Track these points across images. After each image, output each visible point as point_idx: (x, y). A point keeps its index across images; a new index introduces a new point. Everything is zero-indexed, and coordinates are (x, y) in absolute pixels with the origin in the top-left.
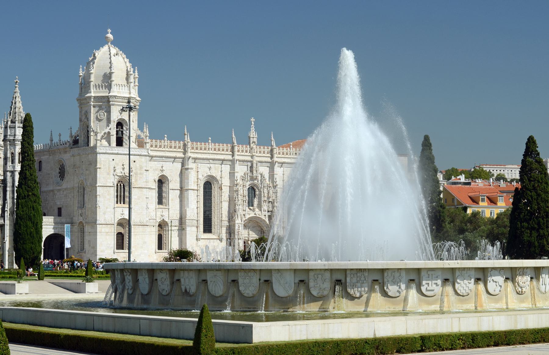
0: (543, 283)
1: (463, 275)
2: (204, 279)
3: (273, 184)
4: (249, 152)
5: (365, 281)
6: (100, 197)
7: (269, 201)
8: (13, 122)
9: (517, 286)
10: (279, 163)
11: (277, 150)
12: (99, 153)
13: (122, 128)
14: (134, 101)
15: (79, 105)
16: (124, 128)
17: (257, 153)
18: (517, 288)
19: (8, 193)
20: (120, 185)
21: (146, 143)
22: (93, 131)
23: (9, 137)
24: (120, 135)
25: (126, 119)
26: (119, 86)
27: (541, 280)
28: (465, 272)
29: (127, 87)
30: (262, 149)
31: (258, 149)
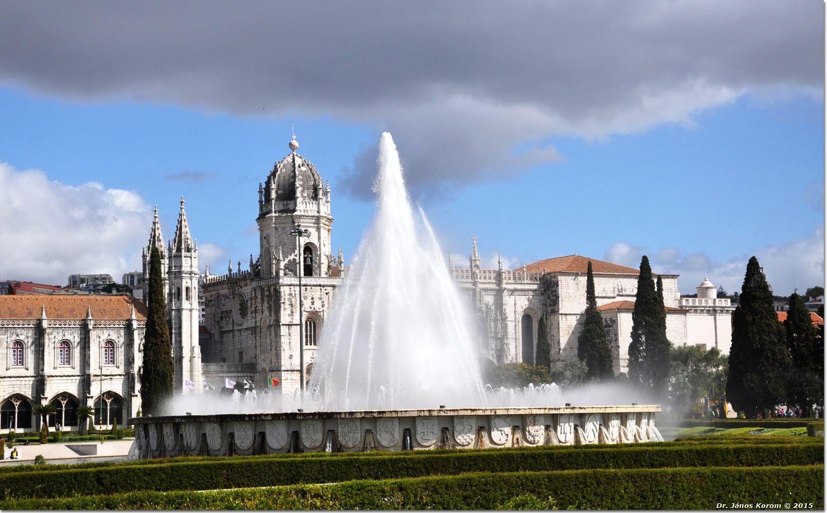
0: (562, 431)
1: (462, 423)
2: (203, 432)
3: (502, 317)
4: (470, 277)
5: (356, 431)
6: (284, 338)
7: (498, 338)
8: (179, 249)
9: (528, 434)
10: (509, 290)
11: (507, 274)
12: (283, 285)
13: (311, 254)
14: (324, 220)
15: (259, 227)
17: (480, 279)
18: (528, 437)
21: (340, 271)
22: (275, 258)
23: (173, 269)
24: (309, 263)
25: (315, 243)
26: (306, 204)
27: (559, 428)
28: (465, 420)
29: (316, 204)
30: (487, 274)
31: (482, 274)
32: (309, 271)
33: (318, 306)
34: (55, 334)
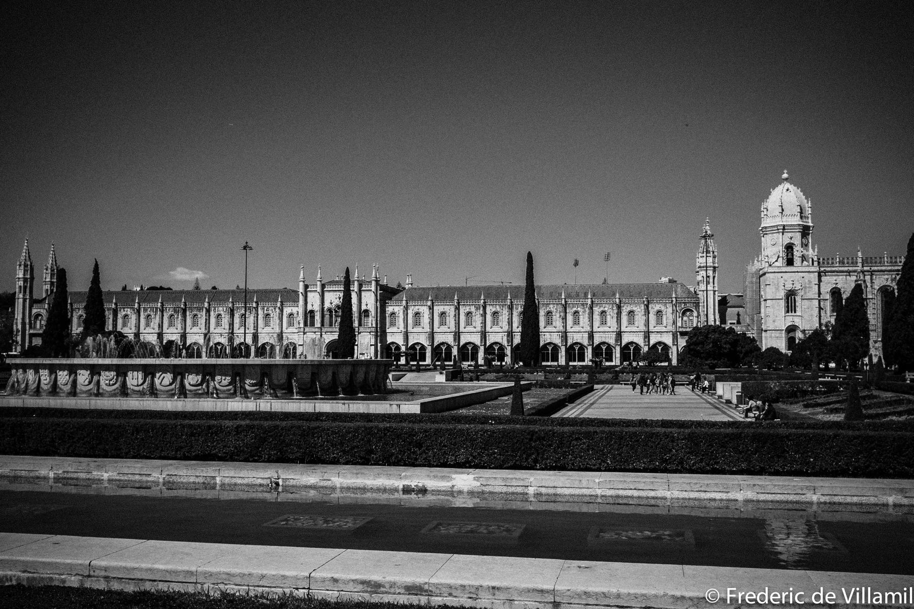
8: (703, 253)
13: (792, 250)
16: (794, 250)
19: (700, 308)
20: (791, 298)
24: (790, 256)
32: (790, 262)
33: (798, 286)
34: (625, 307)
